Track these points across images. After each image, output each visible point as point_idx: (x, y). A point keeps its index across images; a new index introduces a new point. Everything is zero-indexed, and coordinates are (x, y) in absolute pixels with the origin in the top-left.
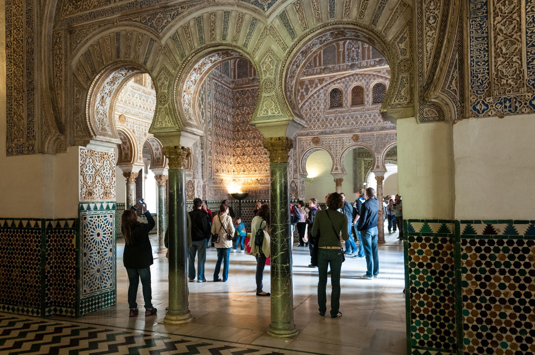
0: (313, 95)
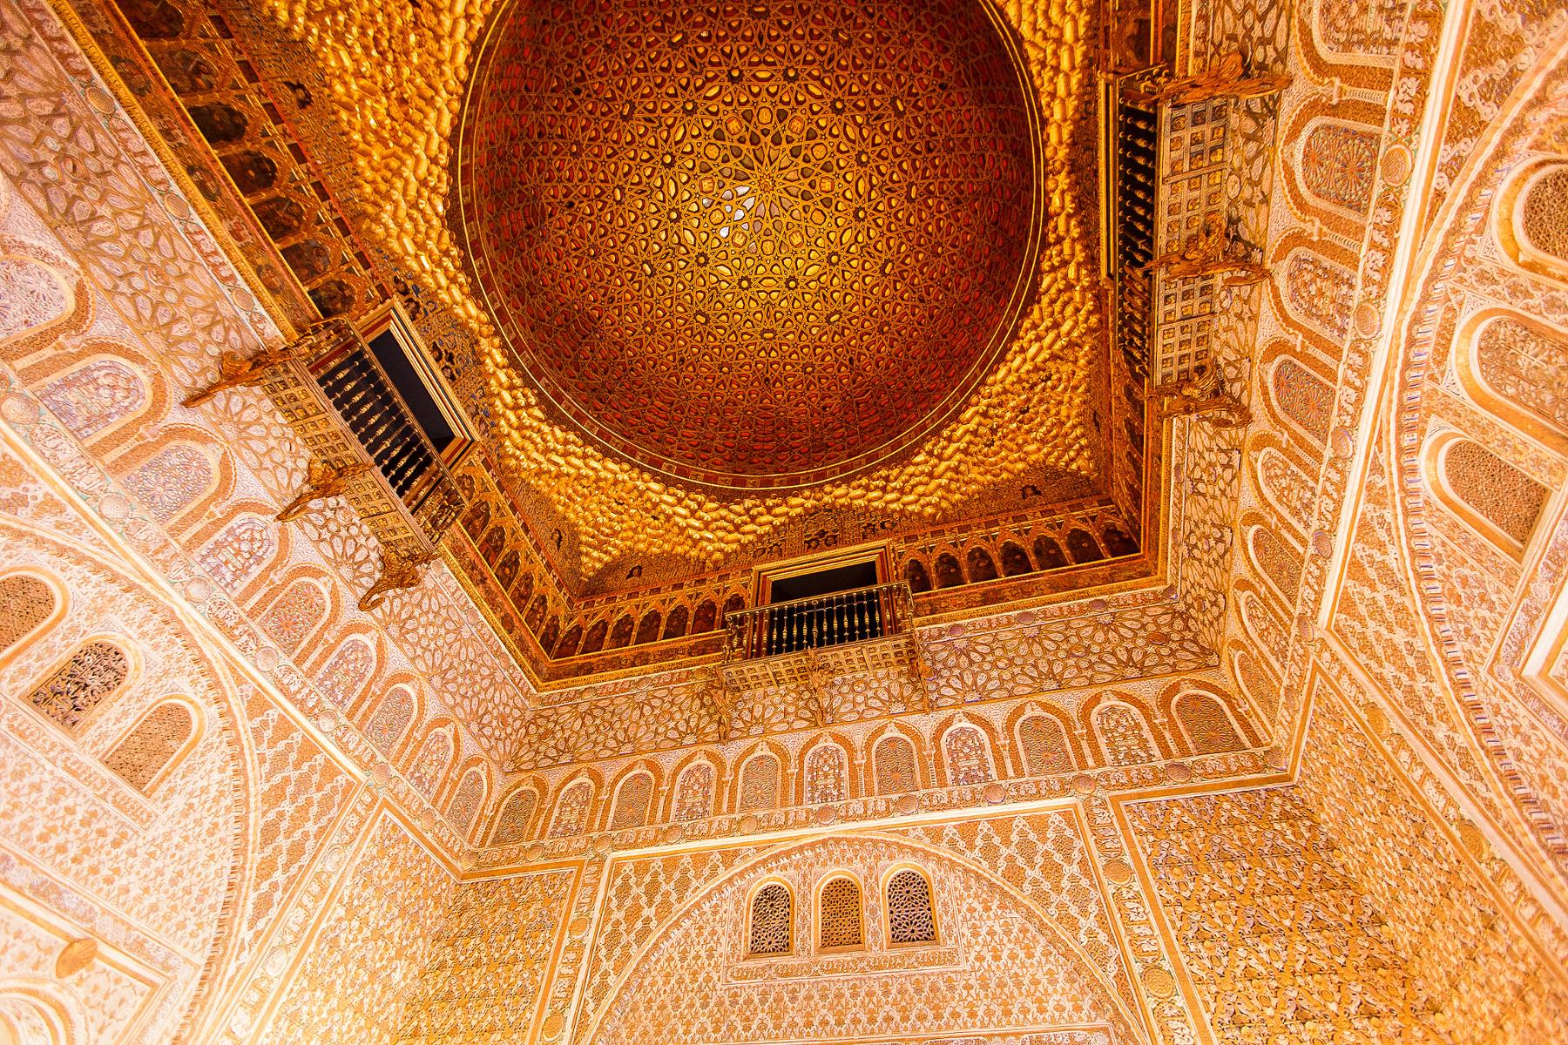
0: (698, 905)
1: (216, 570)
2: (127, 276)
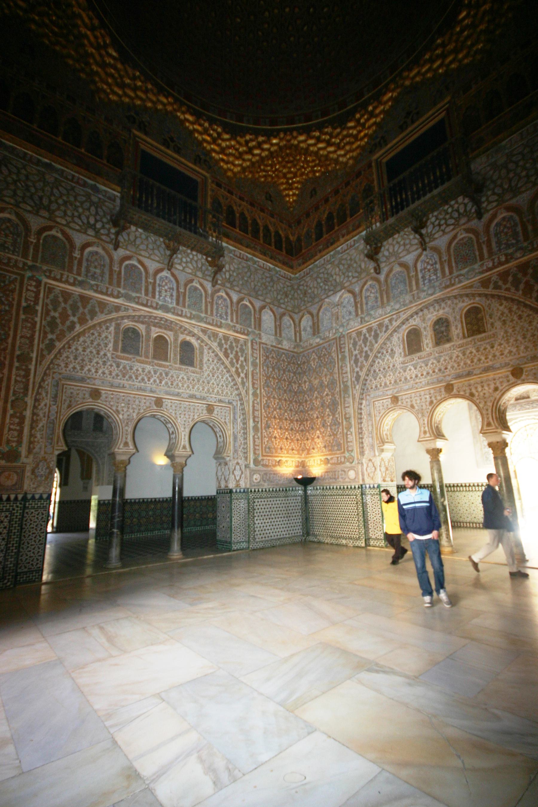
1: (430, 281)
2: (348, 277)
